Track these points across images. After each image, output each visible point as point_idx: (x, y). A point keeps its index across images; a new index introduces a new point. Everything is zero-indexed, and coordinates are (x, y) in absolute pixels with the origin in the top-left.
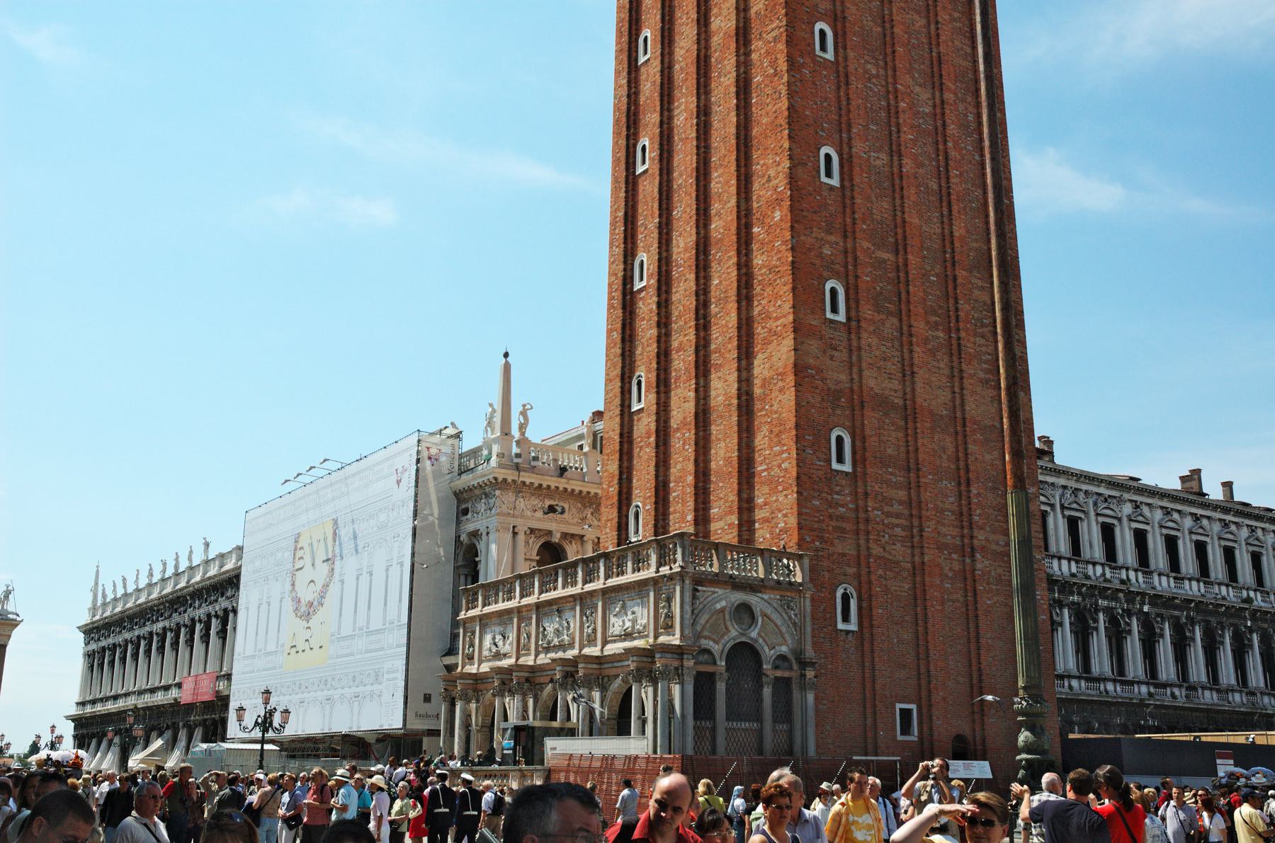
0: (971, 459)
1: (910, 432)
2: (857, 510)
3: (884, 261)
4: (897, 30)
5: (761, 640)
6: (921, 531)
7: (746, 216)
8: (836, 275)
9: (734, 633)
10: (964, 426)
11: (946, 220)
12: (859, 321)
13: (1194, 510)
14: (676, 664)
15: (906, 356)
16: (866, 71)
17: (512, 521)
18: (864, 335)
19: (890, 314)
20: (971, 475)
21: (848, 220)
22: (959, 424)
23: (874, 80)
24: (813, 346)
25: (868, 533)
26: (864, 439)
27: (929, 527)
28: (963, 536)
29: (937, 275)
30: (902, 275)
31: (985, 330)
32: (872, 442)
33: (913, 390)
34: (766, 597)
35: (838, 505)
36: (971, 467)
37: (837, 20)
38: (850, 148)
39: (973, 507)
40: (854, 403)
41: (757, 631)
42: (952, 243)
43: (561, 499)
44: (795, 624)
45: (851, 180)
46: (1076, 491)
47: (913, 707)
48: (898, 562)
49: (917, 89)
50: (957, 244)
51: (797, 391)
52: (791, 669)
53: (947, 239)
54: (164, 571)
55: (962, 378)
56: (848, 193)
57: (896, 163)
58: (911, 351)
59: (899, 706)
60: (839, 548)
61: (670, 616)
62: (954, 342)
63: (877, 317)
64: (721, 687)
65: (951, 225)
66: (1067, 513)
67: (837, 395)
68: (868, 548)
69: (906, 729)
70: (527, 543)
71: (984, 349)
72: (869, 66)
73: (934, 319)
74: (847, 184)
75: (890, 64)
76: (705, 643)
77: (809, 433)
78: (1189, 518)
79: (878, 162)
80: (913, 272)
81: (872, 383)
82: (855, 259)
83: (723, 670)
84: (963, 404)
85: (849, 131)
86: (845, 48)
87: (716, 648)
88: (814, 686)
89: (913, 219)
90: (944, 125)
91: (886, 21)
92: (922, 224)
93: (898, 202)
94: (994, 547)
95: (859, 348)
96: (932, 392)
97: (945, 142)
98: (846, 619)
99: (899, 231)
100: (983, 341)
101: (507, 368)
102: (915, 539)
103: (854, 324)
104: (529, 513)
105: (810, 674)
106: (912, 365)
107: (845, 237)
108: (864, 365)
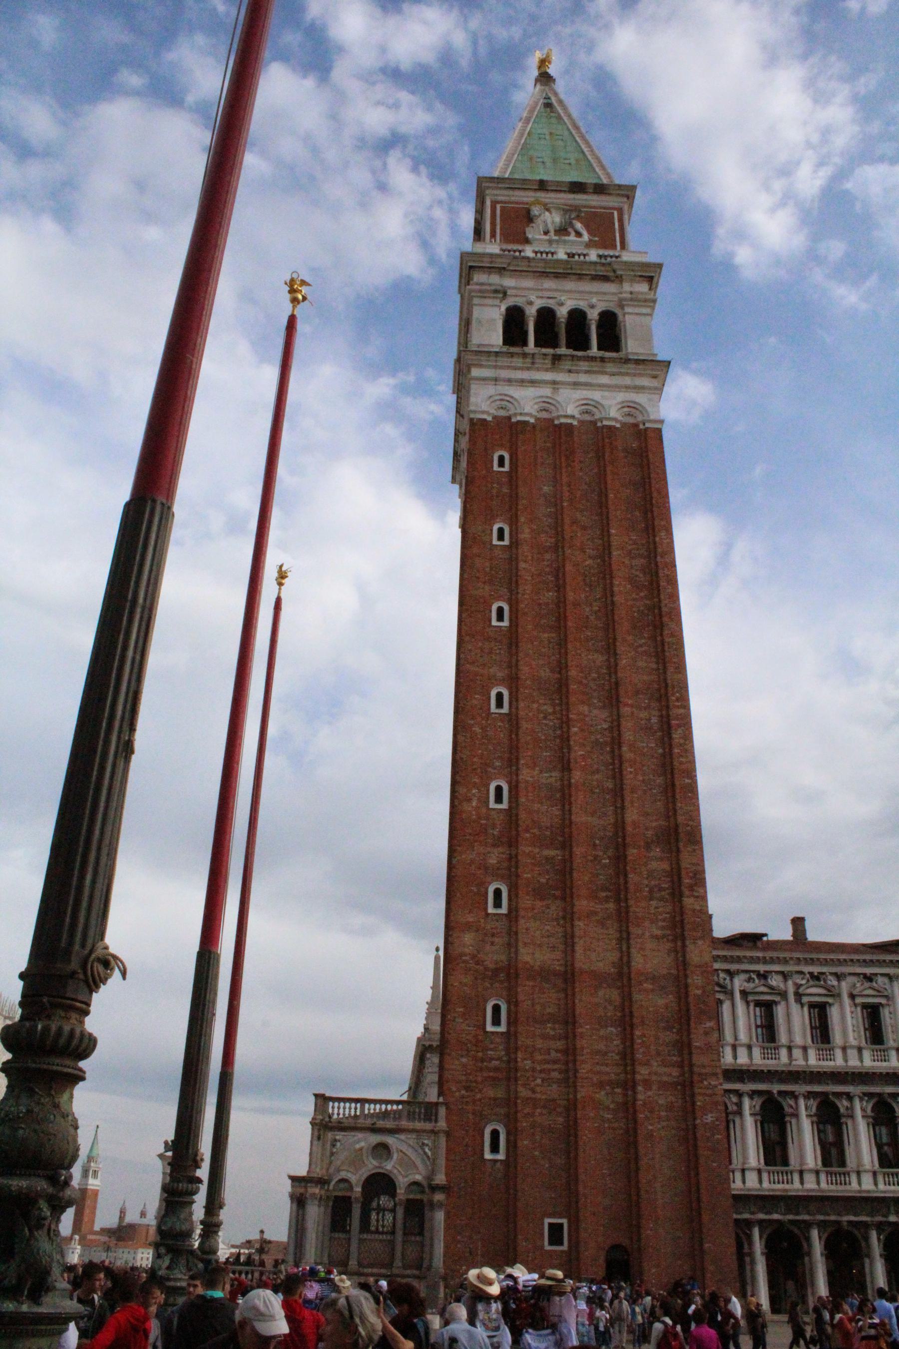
0: (635, 1007)
1: (570, 992)
2: (509, 1062)
3: (553, 858)
4: (573, 673)
5: (395, 1171)
6: (576, 1071)
8: (501, 878)
9: (371, 1165)
11: (619, 811)
18: (522, 922)
19: (556, 898)
20: (635, 1021)
25: (516, 1080)
26: (516, 1005)
27: (584, 1070)
28: (626, 1073)
29: (609, 858)
31: (663, 893)
32: (525, 1005)
34: (402, 1137)
35: (491, 1059)
36: (635, 1014)
37: (513, 682)
39: (636, 1046)
40: (509, 975)
41: (392, 1163)
42: (624, 828)
47: (564, 1221)
48: (554, 1100)
49: (595, 712)
50: (629, 829)
52: (423, 1192)
55: (628, 939)
58: (573, 926)
59: (547, 1221)
60: (491, 1093)
62: (623, 910)
63: (539, 904)
67: (496, 972)
68: (516, 1092)
71: (660, 910)
72: (545, 707)
73: (604, 894)
75: (564, 701)
76: (343, 1174)
80: (577, 861)
81: (528, 958)
83: (359, 1195)
84: (629, 962)
86: (517, 700)
87: (353, 1179)
88: (440, 1205)
90: (620, 735)
91: (561, 667)
93: (567, 807)
94: (665, 1079)
95: (516, 933)
97: (620, 747)
98: (495, 1149)
102: (569, 1078)
105: (439, 1197)
106: (573, 937)
107: (510, 846)
108: (520, 944)
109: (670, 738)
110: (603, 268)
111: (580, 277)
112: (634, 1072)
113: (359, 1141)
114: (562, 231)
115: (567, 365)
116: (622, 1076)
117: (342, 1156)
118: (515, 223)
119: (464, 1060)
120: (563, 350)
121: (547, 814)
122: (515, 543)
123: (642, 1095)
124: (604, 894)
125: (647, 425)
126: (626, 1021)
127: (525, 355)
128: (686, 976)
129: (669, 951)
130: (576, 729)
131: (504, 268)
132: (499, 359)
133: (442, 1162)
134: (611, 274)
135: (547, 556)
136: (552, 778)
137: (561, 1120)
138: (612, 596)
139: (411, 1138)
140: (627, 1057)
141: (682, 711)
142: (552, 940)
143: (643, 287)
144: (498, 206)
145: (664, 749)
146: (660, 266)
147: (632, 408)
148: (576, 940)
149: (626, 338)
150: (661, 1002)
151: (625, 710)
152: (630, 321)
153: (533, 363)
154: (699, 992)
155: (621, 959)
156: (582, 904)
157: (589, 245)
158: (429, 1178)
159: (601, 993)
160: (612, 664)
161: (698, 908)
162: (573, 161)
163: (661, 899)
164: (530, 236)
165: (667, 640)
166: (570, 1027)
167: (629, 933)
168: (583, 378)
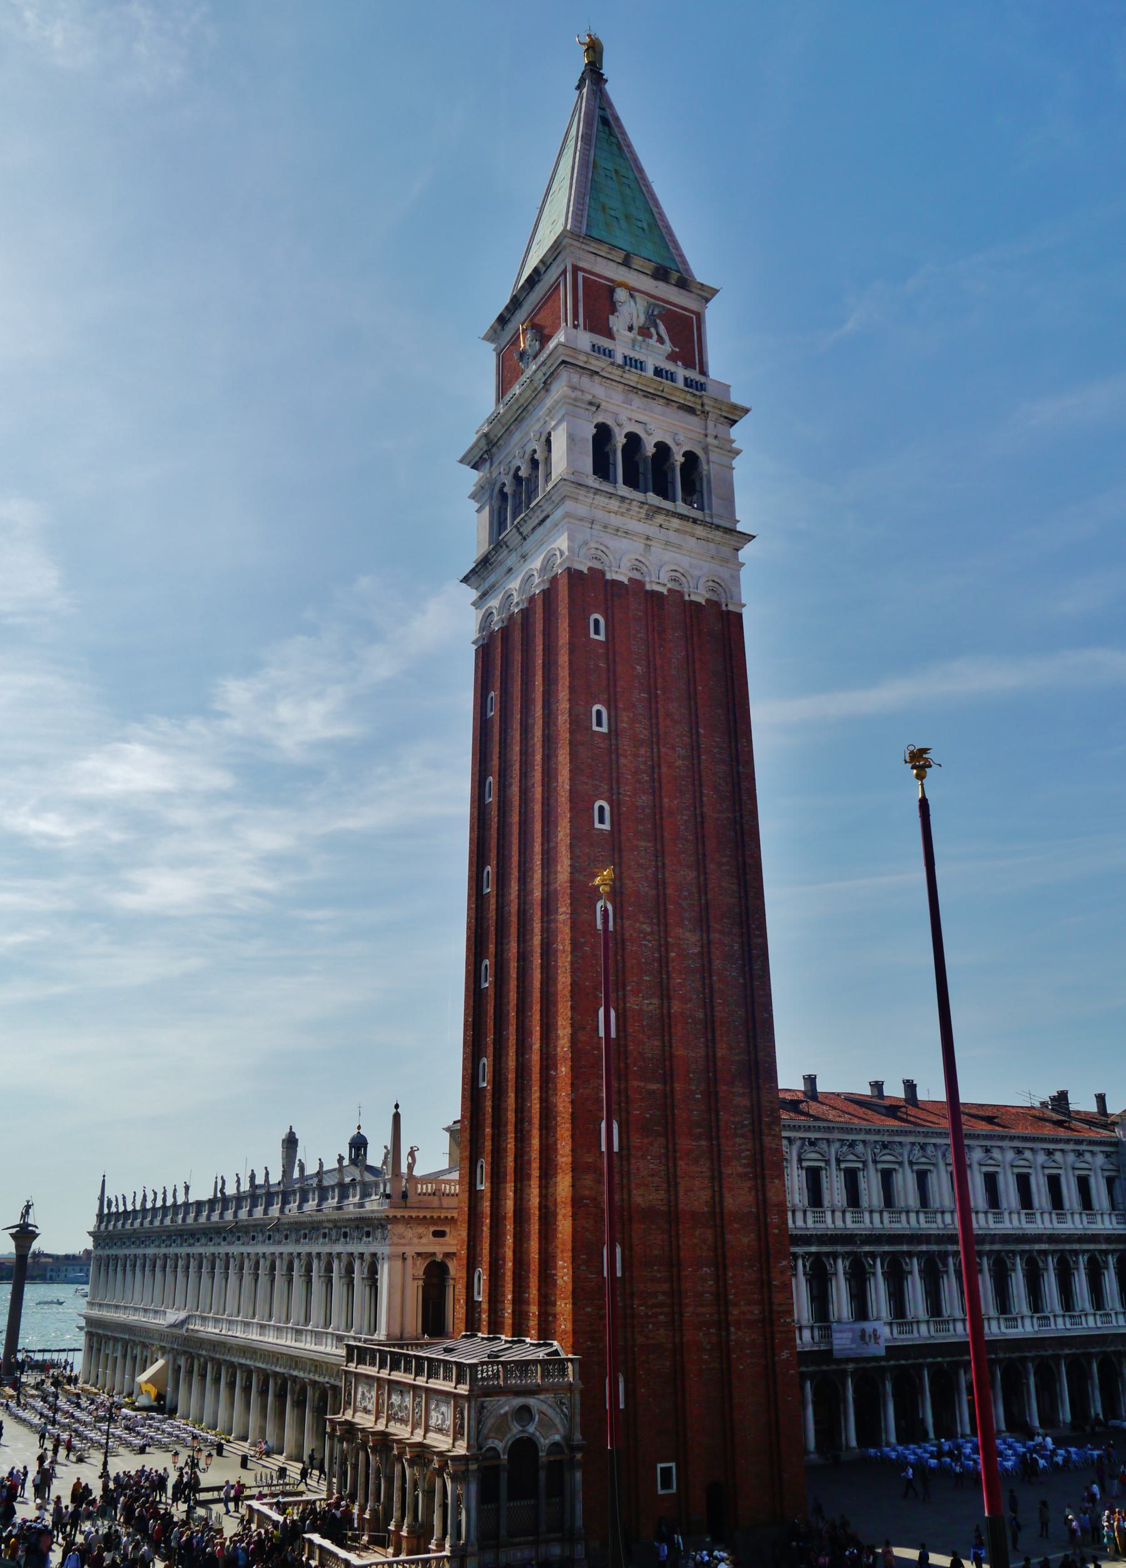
3: (654, 1091)
4: (669, 891)
5: (537, 1433)
6: (681, 1315)
7: (547, 1059)
10: (722, 1218)
12: (629, 1149)
13: (1046, 1146)
14: (463, 1468)
15: (671, 1170)
16: (641, 931)
17: (401, 1249)
18: (633, 1161)
21: (622, 1065)
22: (717, 1217)
23: (648, 937)
24: (588, 1180)
27: (688, 1312)
30: (669, 1101)
33: (677, 1197)
34: (542, 1397)
38: (625, 1003)
40: (622, 1219)
42: (715, 1064)
43: (443, 1225)
44: (565, 1415)
45: (625, 1030)
46: (923, 1147)
47: (673, 1465)
49: (688, 934)
50: (720, 1064)
51: (573, 1220)
52: (563, 1452)
53: (711, 1059)
54: (155, 1200)
55: (720, 1180)
56: (622, 1042)
57: (666, 1005)
58: (675, 1165)
61: (462, 1427)
63: (645, 1141)
64: (504, 1476)
65: (714, 1047)
66: (915, 1167)
69: (666, 1484)
70: (414, 1264)
71: (743, 1147)
72: (644, 926)
73: (698, 1130)
74: (621, 1034)
76: (490, 1443)
77: (585, 1251)
78: (1042, 1152)
79: (651, 1007)
81: (639, 1200)
82: (627, 1097)
83: (505, 1462)
84: (721, 1201)
85: (624, 989)
86: (622, 919)
87: (499, 1445)
89: (680, 1052)
92: (689, 1052)
94: (749, 1317)
95: (629, 1173)
96: (695, 1196)
97: (711, 976)
99: (667, 1063)
100: (742, 1140)
101: (397, 1117)
103: (625, 1152)
104: (416, 1240)
105: (579, 1456)
106: (675, 1176)
108: (633, 1185)
109: (751, 969)
110: (693, 399)
111: (668, 402)
112: (727, 1313)
113: (501, 1407)
114: (644, 332)
115: (660, 519)
116: (716, 1317)
117: (490, 1423)
118: (598, 305)
119: (589, 1309)
120: (653, 498)
121: (651, 1047)
122: (614, 731)
123: (735, 1334)
124: (698, 1130)
125: (731, 608)
126: (720, 1262)
127: (623, 499)
128: (765, 1215)
129: (750, 1189)
130: (673, 954)
131: (597, 373)
132: (597, 497)
133: (578, 1419)
134: (699, 407)
135: (642, 751)
136: (651, 1005)
137: (668, 1364)
138: (702, 806)
139: (549, 1397)
140: (721, 1298)
141: (760, 940)
142: (657, 1179)
143: (721, 429)
144: (580, 274)
145: (745, 979)
146: (746, 411)
147: (716, 585)
148: (679, 1180)
149: (710, 492)
150: (746, 1240)
151: (715, 936)
152: (710, 468)
153: (628, 510)
154: (776, 1231)
155: (713, 1198)
156: (684, 1143)
157: (672, 357)
158: (568, 1438)
159: (697, 1233)
160: (702, 882)
161: (774, 1146)
162: (645, 227)
163: (743, 1136)
164: (615, 329)
165: (749, 861)
166: (675, 1269)
167: (720, 1173)
168: (673, 536)
